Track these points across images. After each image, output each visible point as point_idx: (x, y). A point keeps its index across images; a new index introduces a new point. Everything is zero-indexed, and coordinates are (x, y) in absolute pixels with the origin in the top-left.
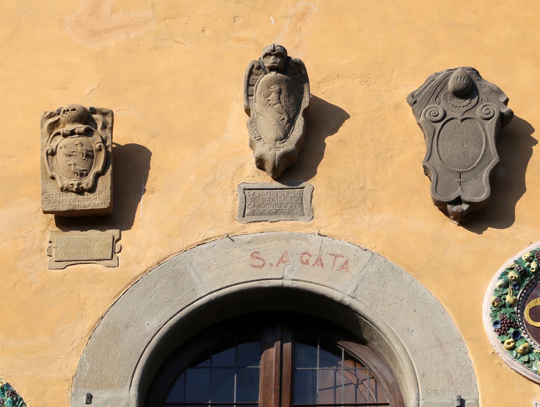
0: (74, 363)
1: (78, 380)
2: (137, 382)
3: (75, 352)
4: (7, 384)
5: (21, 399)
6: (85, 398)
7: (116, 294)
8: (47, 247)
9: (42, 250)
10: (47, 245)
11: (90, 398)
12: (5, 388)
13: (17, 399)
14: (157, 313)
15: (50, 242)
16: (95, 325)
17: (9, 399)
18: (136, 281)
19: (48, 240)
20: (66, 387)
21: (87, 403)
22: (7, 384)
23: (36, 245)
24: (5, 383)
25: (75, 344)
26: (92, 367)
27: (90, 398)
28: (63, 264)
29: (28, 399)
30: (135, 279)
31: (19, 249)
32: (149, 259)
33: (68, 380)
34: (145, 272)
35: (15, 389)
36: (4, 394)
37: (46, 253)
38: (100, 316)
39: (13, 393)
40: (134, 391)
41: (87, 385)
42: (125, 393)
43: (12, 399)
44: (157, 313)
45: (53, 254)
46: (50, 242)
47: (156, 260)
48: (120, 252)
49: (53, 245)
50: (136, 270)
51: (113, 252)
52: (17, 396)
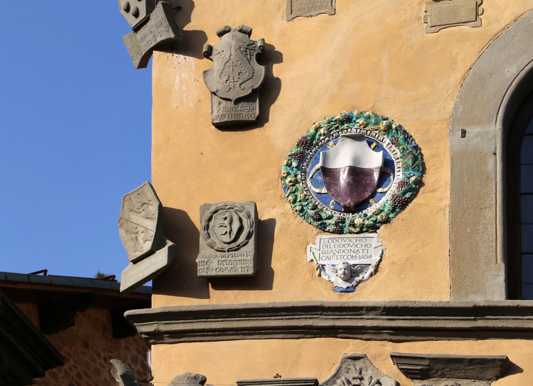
0: (450, 106)
1: (454, 119)
2: (502, 119)
3: (450, 97)
4: (400, 125)
5: (411, 136)
6: (460, 133)
7: (480, 49)
8: (423, 16)
9: (420, 19)
10: (423, 14)
11: (464, 133)
12: (399, 129)
13: (408, 136)
14: (515, 61)
15: (426, 12)
16: (465, 75)
17: (402, 137)
18: (496, 36)
19: (424, 10)
20: (445, 126)
21: (462, 137)
22: (400, 125)
23: (414, 16)
24: (398, 124)
25: (450, 92)
26: (464, 109)
27: (464, 133)
28: (437, 28)
29: (416, 136)
30: (496, 35)
31: (402, 19)
32: (507, 18)
33: (445, 120)
34: (504, 29)
35: (406, 129)
36: (397, 133)
37: (423, 21)
38: (468, 67)
39: (405, 132)
40: (499, 126)
41: (461, 123)
42: (492, 128)
43: (404, 136)
44: (515, 61)
45: (429, 21)
46: (426, 12)
47: (513, 18)
48: (482, 14)
49: (428, 14)
50: (496, 27)
51: (477, 15)
52: (408, 134)
